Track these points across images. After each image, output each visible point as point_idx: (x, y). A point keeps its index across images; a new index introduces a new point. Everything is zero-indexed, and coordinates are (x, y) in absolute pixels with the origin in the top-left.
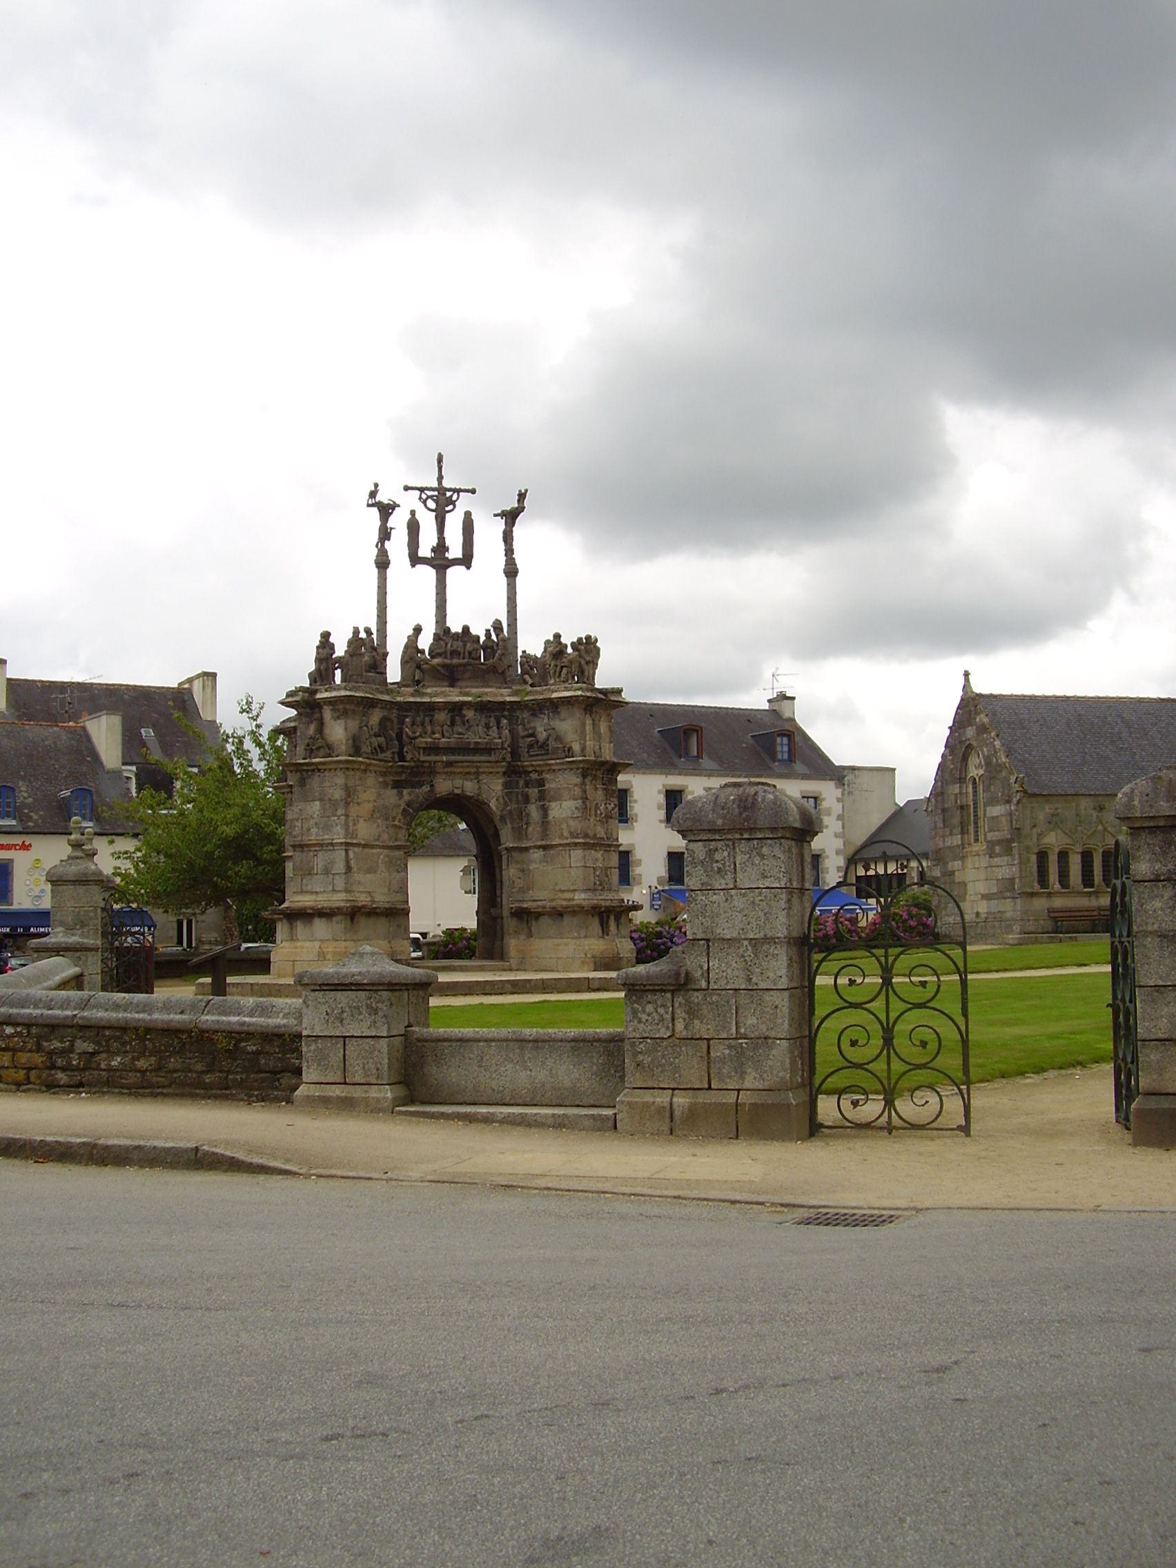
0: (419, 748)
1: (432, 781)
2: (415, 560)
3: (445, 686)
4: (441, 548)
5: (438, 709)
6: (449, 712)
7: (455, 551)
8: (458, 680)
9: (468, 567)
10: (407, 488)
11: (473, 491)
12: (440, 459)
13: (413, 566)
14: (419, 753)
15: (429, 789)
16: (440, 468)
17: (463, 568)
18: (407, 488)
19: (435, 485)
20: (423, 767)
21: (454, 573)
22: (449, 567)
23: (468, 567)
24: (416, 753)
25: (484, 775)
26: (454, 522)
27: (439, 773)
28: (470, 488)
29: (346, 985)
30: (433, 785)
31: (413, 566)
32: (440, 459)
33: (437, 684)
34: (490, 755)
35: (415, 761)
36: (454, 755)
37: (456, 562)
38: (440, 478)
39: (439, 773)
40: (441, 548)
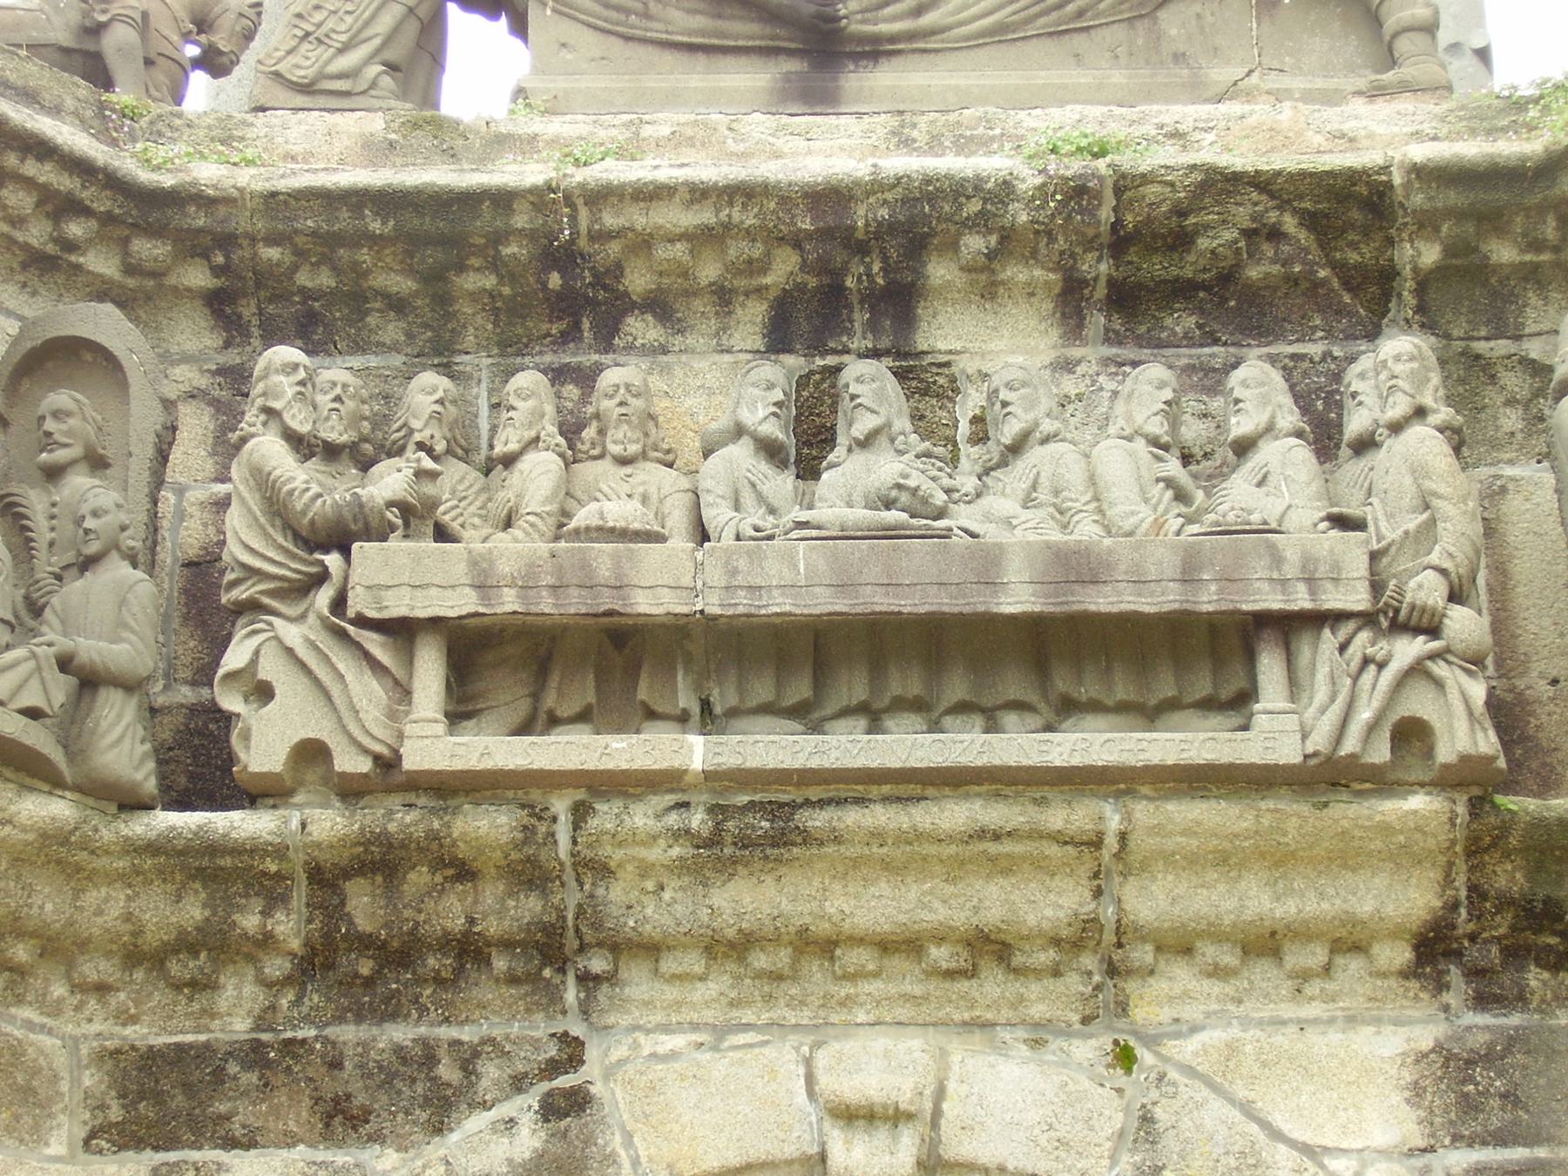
0: (402, 631)
1: (571, 1053)
3: (712, 98)
5: (659, 306)
6: (778, 340)
8: (875, 51)
14: (403, 692)
15: (528, 1140)
20: (463, 872)
24: (367, 692)
25: (1180, 976)
27: (652, 949)
30: (577, 1102)
33: (651, 82)
34: (1240, 702)
35: (350, 791)
36: (807, 716)
39: (652, 949)
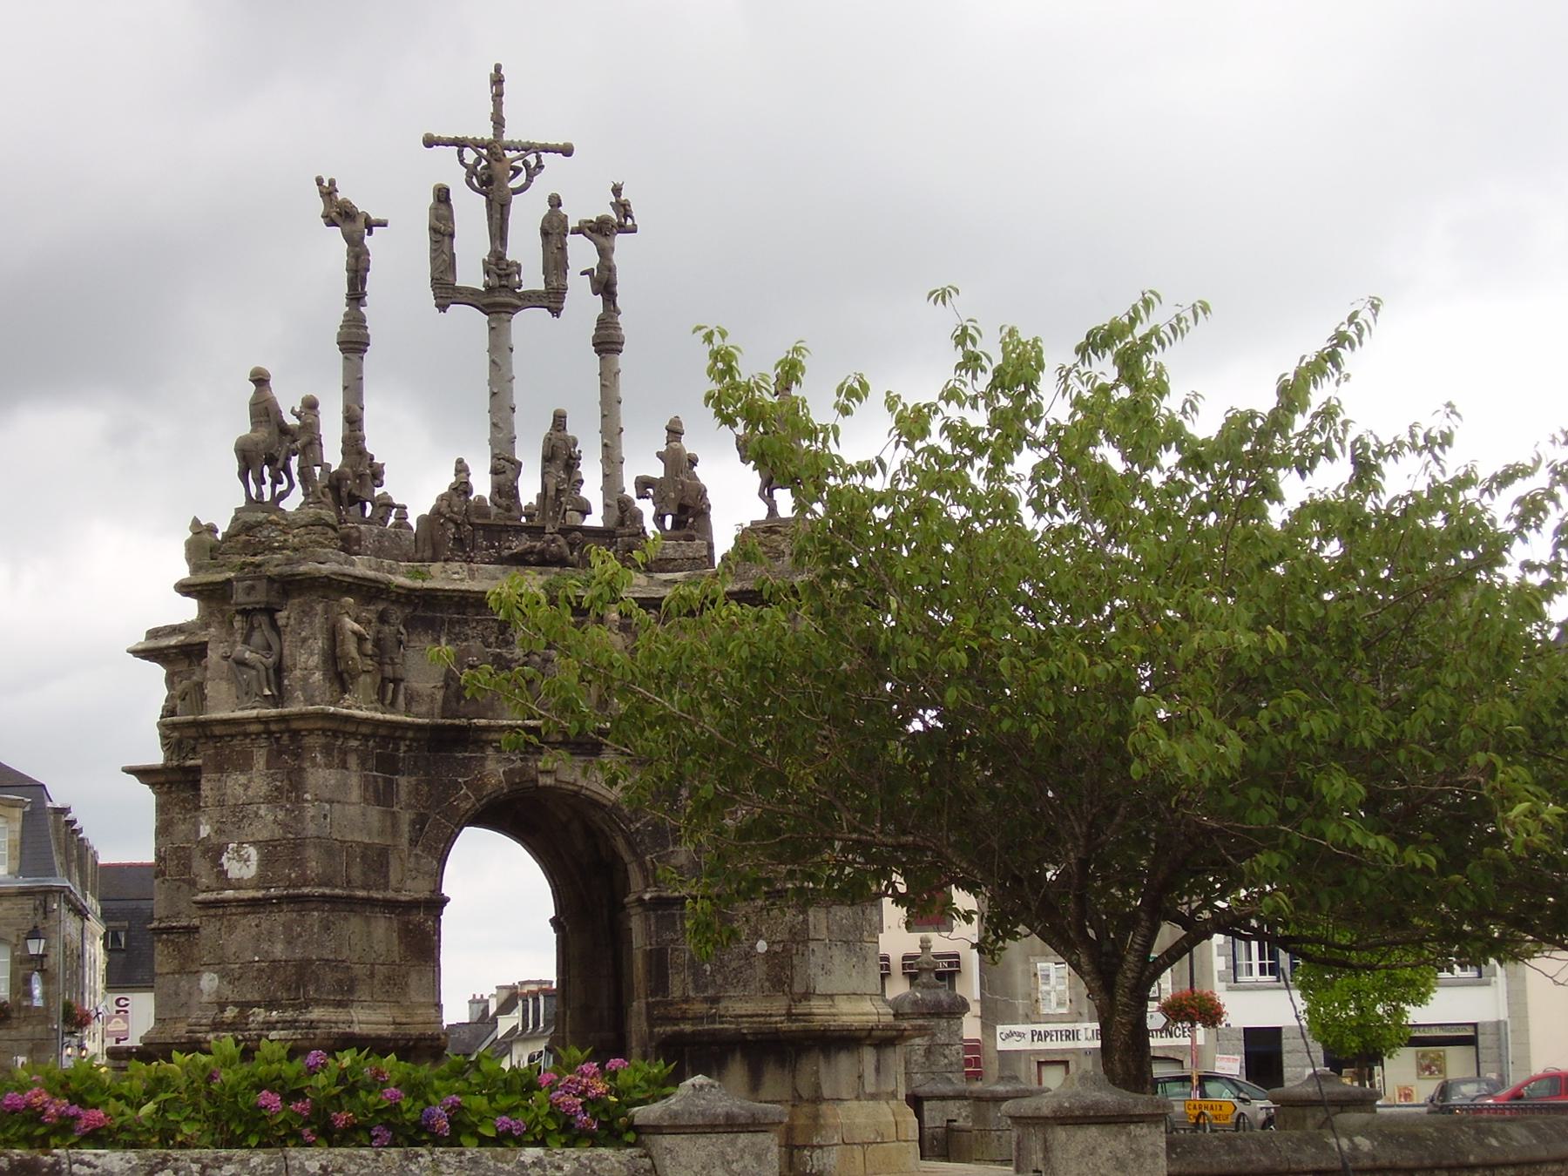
2: (446, 292)
4: (500, 267)
7: (532, 279)
9: (556, 312)
10: (430, 142)
11: (567, 151)
12: (497, 80)
13: (442, 307)
16: (498, 97)
18: (430, 142)
19: (488, 134)
21: (527, 324)
22: (517, 308)
23: (556, 312)
26: (526, 214)
29: (683, 1126)
31: (442, 307)
32: (497, 80)
37: (532, 299)
38: (498, 122)
40: (500, 267)
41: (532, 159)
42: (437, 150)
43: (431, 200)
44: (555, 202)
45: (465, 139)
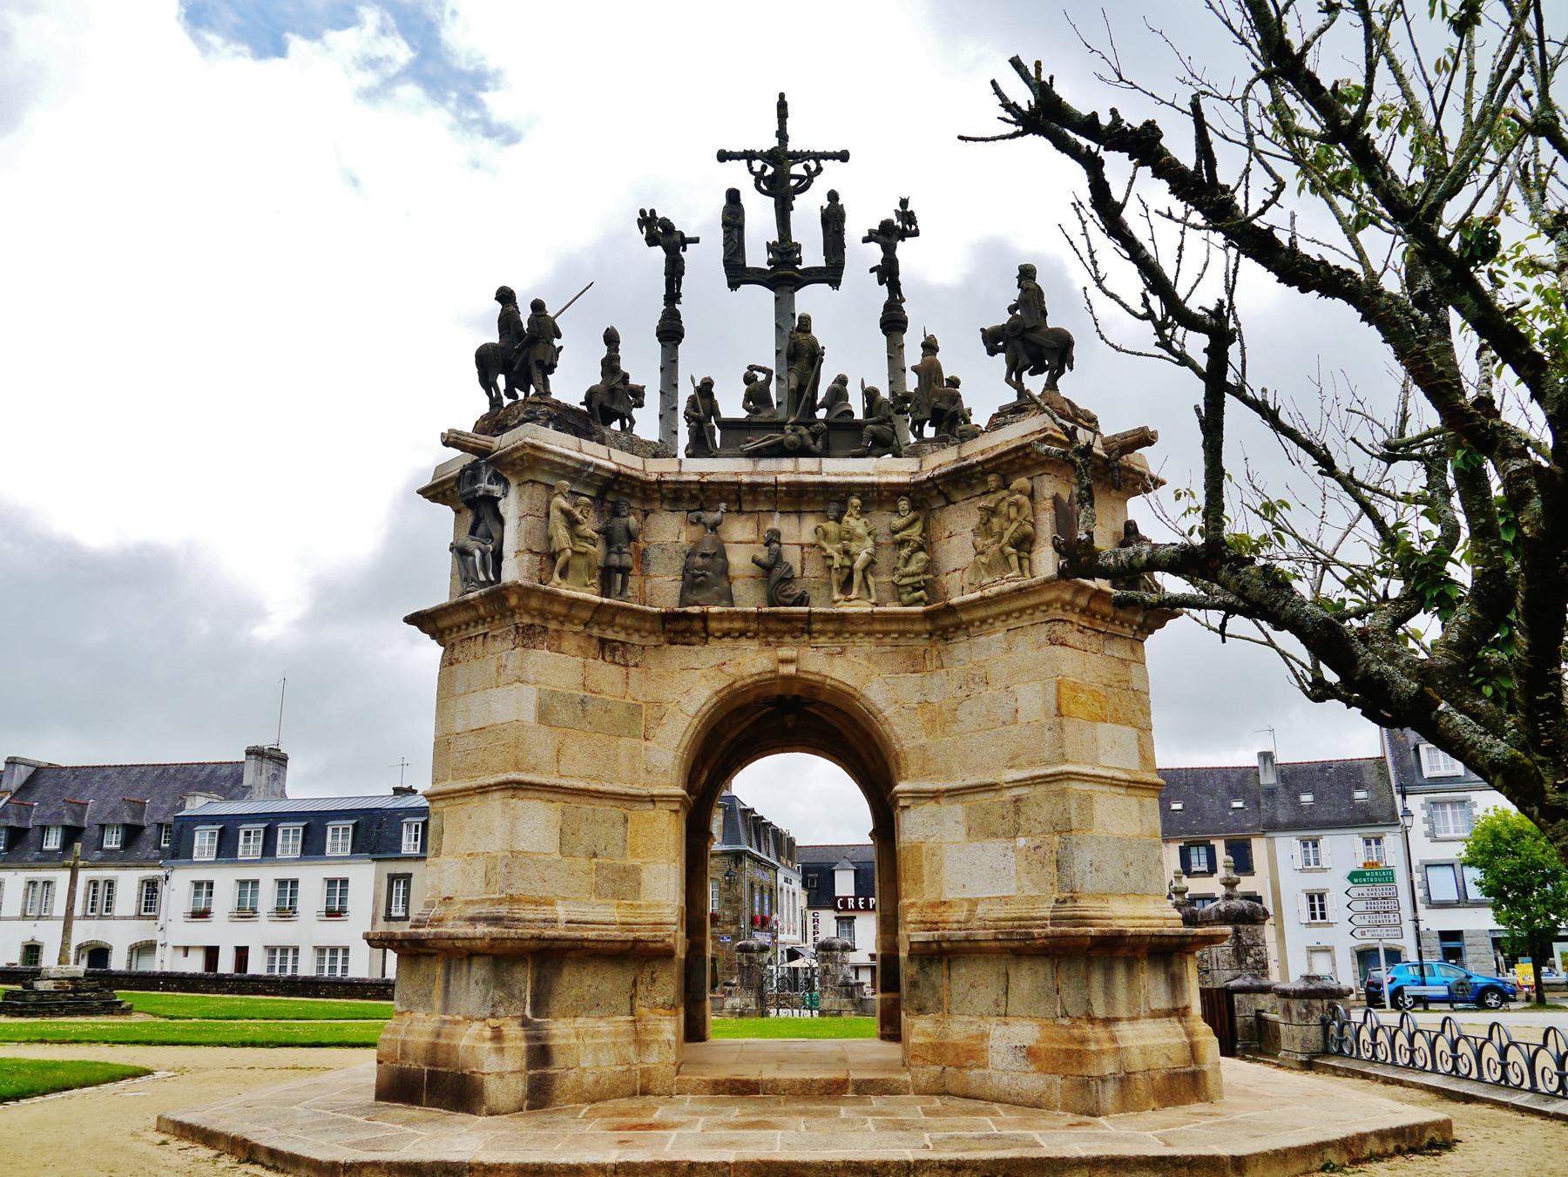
2: (737, 273)
4: (784, 251)
7: (812, 255)
9: (835, 282)
10: (723, 156)
11: (843, 156)
12: (782, 107)
13: (733, 285)
17: (825, 288)
18: (723, 156)
21: (809, 299)
23: (835, 282)
26: (808, 208)
28: (838, 151)
31: (733, 285)
32: (782, 107)
37: (814, 276)
38: (782, 135)
40: (784, 251)
41: (812, 165)
42: (731, 164)
43: (723, 202)
44: (833, 196)
45: (752, 152)
